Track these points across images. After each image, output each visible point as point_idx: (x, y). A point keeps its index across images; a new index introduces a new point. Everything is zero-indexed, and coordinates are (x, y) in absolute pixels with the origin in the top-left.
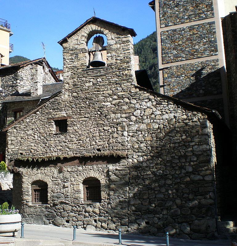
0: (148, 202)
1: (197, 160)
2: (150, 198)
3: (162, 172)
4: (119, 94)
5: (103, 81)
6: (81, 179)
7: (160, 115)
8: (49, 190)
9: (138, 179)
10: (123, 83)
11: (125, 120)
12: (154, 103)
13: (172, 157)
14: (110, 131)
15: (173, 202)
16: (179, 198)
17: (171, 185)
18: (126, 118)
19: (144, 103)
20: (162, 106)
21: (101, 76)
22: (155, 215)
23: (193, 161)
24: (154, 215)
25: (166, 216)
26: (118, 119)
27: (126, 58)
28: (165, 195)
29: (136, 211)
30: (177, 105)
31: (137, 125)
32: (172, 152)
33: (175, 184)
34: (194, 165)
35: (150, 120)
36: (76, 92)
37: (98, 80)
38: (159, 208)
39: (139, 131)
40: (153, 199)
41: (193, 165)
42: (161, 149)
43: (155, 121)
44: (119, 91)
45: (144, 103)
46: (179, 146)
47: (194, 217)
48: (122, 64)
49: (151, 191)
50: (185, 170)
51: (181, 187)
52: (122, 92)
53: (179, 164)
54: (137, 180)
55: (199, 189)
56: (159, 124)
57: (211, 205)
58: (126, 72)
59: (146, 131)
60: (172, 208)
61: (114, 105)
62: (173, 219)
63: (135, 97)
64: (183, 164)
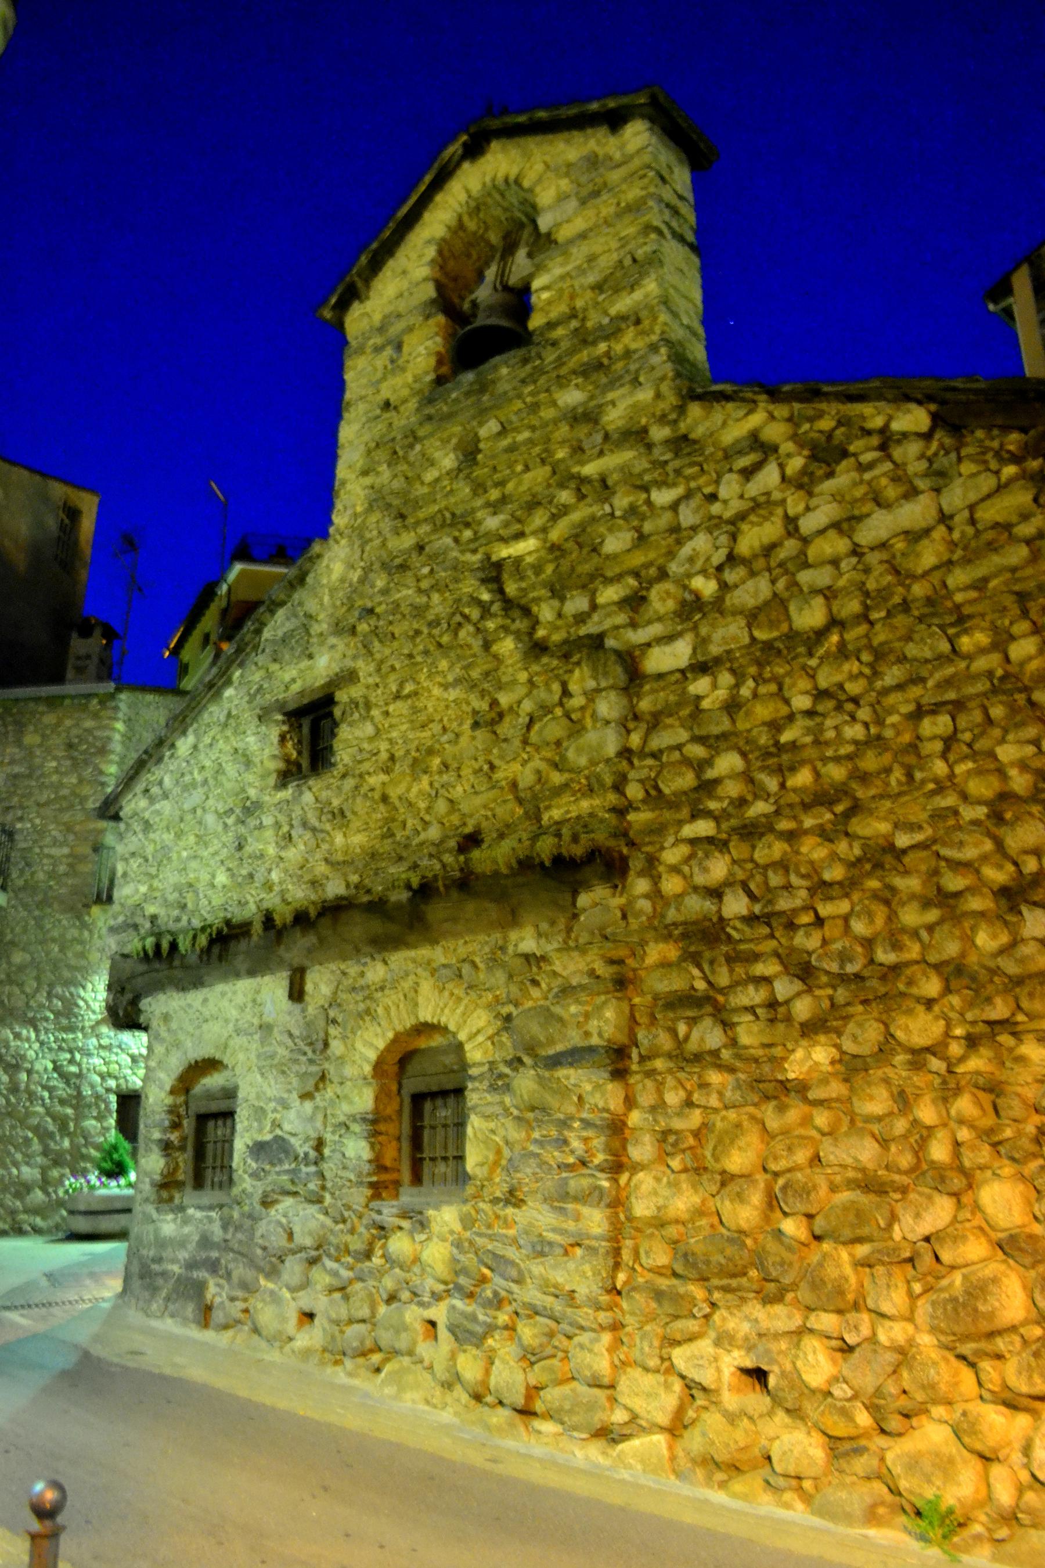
9: (693, 1021)
11: (621, 618)
12: (795, 464)
13: (938, 816)
14: (527, 706)
15: (959, 1204)
16: (1008, 1170)
17: (934, 1054)
19: (730, 488)
20: (852, 460)
22: (813, 1317)
30: (957, 429)
32: (936, 781)
33: (972, 1042)
35: (773, 582)
39: (702, 667)
43: (805, 577)
52: (601, 453)
53: (997, 875)
62: (962, 1358)
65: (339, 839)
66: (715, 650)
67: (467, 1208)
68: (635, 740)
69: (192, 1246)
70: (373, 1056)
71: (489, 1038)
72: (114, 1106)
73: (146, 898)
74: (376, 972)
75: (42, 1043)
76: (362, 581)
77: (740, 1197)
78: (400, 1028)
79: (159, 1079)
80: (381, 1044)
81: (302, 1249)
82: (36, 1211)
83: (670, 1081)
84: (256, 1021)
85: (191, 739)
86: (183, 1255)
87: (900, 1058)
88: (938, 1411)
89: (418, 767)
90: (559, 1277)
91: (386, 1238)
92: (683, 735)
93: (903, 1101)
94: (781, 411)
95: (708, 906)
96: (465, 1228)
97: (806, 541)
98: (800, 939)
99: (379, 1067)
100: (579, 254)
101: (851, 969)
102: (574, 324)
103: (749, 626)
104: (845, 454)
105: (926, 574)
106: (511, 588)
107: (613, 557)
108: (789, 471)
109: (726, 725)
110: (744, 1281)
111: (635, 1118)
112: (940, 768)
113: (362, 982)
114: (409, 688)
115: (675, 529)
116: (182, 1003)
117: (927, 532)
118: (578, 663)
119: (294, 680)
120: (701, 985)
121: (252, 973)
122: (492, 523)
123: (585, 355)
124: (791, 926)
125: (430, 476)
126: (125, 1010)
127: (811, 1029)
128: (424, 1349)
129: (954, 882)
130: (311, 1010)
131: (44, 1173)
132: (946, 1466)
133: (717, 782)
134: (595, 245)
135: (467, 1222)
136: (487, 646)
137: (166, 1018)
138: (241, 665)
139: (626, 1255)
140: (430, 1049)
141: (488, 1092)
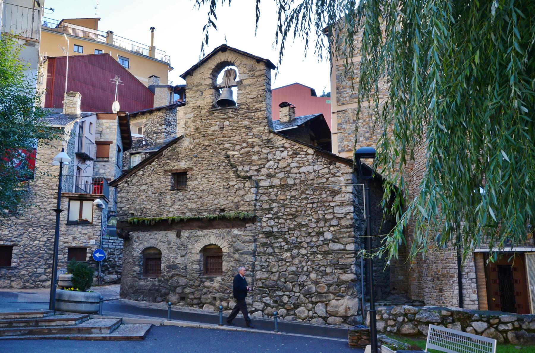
0: (277, 276)
1: (339, 224)
4: (249, 140)
6: (199, 246)
7: (297, 167)
8: (163, 260)
9: (267, 248)
11: (256, 173)
12: (290, 153)
13: (309, 220)
14: (236, 186)
18: (256, 170)
19: (278, 153)
20: (300, 156)
21: (230, 118)
23: (333, 226)
24: (284, 292)
25: (298, 294)
26: (247, 172)
27: (259, 96)
28: (298, 268)
29: (263, 287)
30: (317, 155)
31: (269, 180)
33: (311, 254)
34: (335, 231)
35: (285, 174)
37: (225, 123)
39: (271, 187)
41: (333, 231)
43: (290, 175)
44: (249, 137)
45: (278, 153)
46: (317, 207)
47: (332, 296)
48: (254, 104)
49: (282, 263)
50: (324, 236)
51: (318, 258)
54: (265, 249)
55: (338, 261)
56: (295, 179)
57: (353, 281)
60: (305, 284)
61: (242, 154)
64: (321, 230)
65: (189, 204)
66: (274, 184)
67: (223, 277)
68: (258, 198)
70: (200, 249)
72: (67, 251)
73: (129, 208)
74: (199, 233)
75: (44, 233)
76: (194, 148)
77: (274, 276)
80: (202, 247)
81: (181, 285)
82: (43, 281)
83: (263, 257)
84: (166, 240)
85: (141, 173)
87: (301, 256)
88: (303, 305)
89: (210, 194)
92: (267, 198)
93: (301, 262)
94: (289, 141)
95: (271, 229)
97: (291, 169)
98: (286, 236)
99: (201, 251)
100: (248, 90)
101: (294, 242)
102: (247, 106)
104: (299, 154)
105: (311, 180)
106: (232, 160)
107: (254, 161)
109: (275, 198)
111: (256, 263)
112: (309, 212)
113: (195, 235)
114: (207, 176)
115: (267, 158)
117: (312, 173)
119: (174, 166)
121: (165, 230)
122: (227, 145)
123: (249, 114)
124: (285, 234)
125: (212, 129)
127: (287, 251)
128: (213, 302)
129: (310, 230)
130: (183, 239)
132: (304, 312)
133: (273, 208)
134: (251, 88)
135: (223, 280)
136: (227, 172)
137: (138, 237)
138: (157, 158)
139: (255, 285)
140: (210, 248)
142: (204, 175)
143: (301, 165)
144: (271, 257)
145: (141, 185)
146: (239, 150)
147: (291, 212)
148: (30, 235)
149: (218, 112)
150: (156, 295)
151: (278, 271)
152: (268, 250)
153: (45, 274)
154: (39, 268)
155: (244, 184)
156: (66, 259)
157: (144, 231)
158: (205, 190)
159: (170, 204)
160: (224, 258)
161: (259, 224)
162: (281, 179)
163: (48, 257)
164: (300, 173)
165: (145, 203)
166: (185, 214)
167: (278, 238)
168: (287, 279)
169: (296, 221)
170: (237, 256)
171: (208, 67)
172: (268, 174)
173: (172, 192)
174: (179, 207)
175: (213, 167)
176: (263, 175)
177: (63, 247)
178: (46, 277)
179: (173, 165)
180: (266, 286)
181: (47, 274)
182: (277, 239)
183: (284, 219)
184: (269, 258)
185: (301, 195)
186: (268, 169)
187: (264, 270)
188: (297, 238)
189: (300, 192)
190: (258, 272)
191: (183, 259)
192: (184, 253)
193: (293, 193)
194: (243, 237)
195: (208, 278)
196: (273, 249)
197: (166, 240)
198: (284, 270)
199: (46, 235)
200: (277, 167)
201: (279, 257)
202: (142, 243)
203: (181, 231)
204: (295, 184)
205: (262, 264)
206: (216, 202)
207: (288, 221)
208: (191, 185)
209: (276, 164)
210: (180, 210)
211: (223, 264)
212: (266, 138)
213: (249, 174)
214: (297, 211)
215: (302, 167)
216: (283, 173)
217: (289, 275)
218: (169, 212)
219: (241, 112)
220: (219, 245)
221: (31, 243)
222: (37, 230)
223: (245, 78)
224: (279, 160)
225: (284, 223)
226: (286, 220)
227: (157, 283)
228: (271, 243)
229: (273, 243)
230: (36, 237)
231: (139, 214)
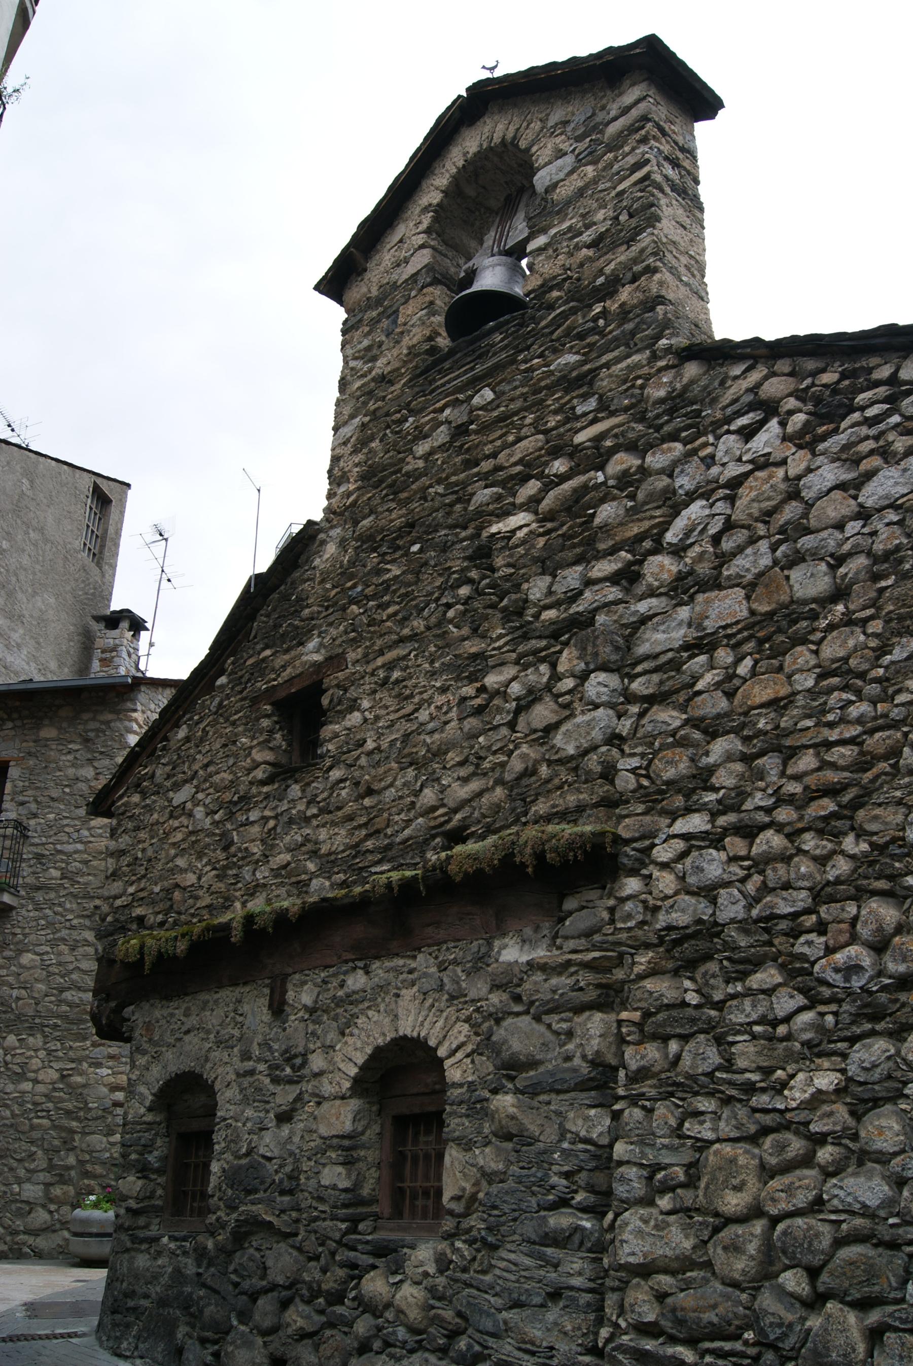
0: (752, 1248)
2: (773, 1211)
3: (867, 959)
4: (580, 438)
5: (503, 393)
7: (841, 486)
8: (219, 1138)
9: (685, 1038)
10: (607, 365)
11: (613, 593)
12: (799, 419)
14: (516, 689)
18: (614, 579)
20: (856, 416)
27: (623, 218)
31: (684, 613)
35: (774, 548)
36: (371, 512)
37: (476, 400)
38: (852, 1318)
40: (799, 1221)
42: (862, 753)
43: (806, 542)
44: (579, 425)
56: (840, 560)
58: (625, 294)
59: (745, 634)
61: (549, 517)
63: (678, 422)
65: (323, 834)
66: (710, 625)
68: (625, 726)
69: (164, 1280)
70: (353, 1071)
71: (468, 1056)
74: (357, 981)
75: (50, 1052)
76: (352, 563)
77: (734, 1248)
78: (380, 1041)
79: (141, 1094)
80: (360, 1059)
81: (274, 1287)
82: (35, 1233)
83: (661, 1109)
85: (182, 733)
86: (156, 1290)
90: (536, 1332)
91: (360, 1278)
95: (704, 909)
96: (441, 1272)
97: (809, 506)
98: (800, 948)
99: (360, 1086)
101: (857, 983)
103: (748, 597)
107: (605, 528)
108: (790, 429)
109: (723, 704)
110: (738, 1346)
111: (620, 1149)
113: (340, 993)
114: (396, 674)
115: (668, 494)
116: (165, 1012)
118: (566, 644)
119: (284, 667)
120: (693, 998)
124: (795, 933)
125: (422, 448)
126: (108, 1017)
131: (47, 1192)
133: (711, 770)
135: (443, 1263)
136: (475, 630)
137: (148, 1027)
139: (610, 1311)
141: (467, 1116)
142: (382, 674)
143: (865, 465)
144: (705, 1104)
145: (177, 787)
146: (532, 504)
147: (832, 776)
148: (9, 1058)
149: (447, 365)
150: (182, 1331)
151: (755, 1212)
152: (686, 1062)
153: (44, 1206)
154: (28, 1180)
155: (554, 666)
156: (116, 1152)
157: (168, 998)
158: (385, 745)
159: (256, 849)
160: (456, 1124)
161: (632, 885)
162: (750, 588)
163: (56, 1142)
164: (864, 515)
165: (181, 862)
166: (302, 886)
167: (757, 964)
168: (824, 1277)
169: (861, 833)
170: (506, 1102)
171: (418, 210)
172: (680, 577)
173: (265, 789)
174: (288, 857)
175: (418, 624)
176: (652, 593)
177: (108, 1103)
178: (47, 1216)
179: (279, 662)
180: (680, 1322)
181: (53, 1207)
182: (743, 976)
183: (779, 827)
184: (697, 1114)
185: (883, 649)
186: (678, 551)
187: (665, 1202)
188: (879, 947)
189: (876, 626)
190: (633, 1218)
191: (285, 1130)
192: (284, 1096)
193: (832, 650)
194: (539, 977)
195: (382, 1251)
196: (719, 1041)
197: (236, 1032)
198: (802, 1199)
199: (58, 1059)
200: (729, 526)
201: (762, 1100)
202: (156, 1057)
203: (285, 978)
204: (840, 594)
205: (651, 1156)
206: (429, 796)
207: (809, 842)
208: (336, 735)
209: (720, 507)
210: (289, 876)
211: (447, 1159)
212: (662, 393)
213: (579, 607)
214: (862, 765)
215: (869, 475)
216: (764, 546)
217: (839, 1243)
218: (253, 890)
219: (543, 323)
220: (432, 1043)
221: (10, 1088)
222: (31, 1039)
223: (562, 175)
224: (736, 483)
225: (786, 859)
226: (789, 836)
227: (190, 1268)
228: (707, 1001)
229: (719, 1006)
230: (23, 1065)
231: (160, 918)
